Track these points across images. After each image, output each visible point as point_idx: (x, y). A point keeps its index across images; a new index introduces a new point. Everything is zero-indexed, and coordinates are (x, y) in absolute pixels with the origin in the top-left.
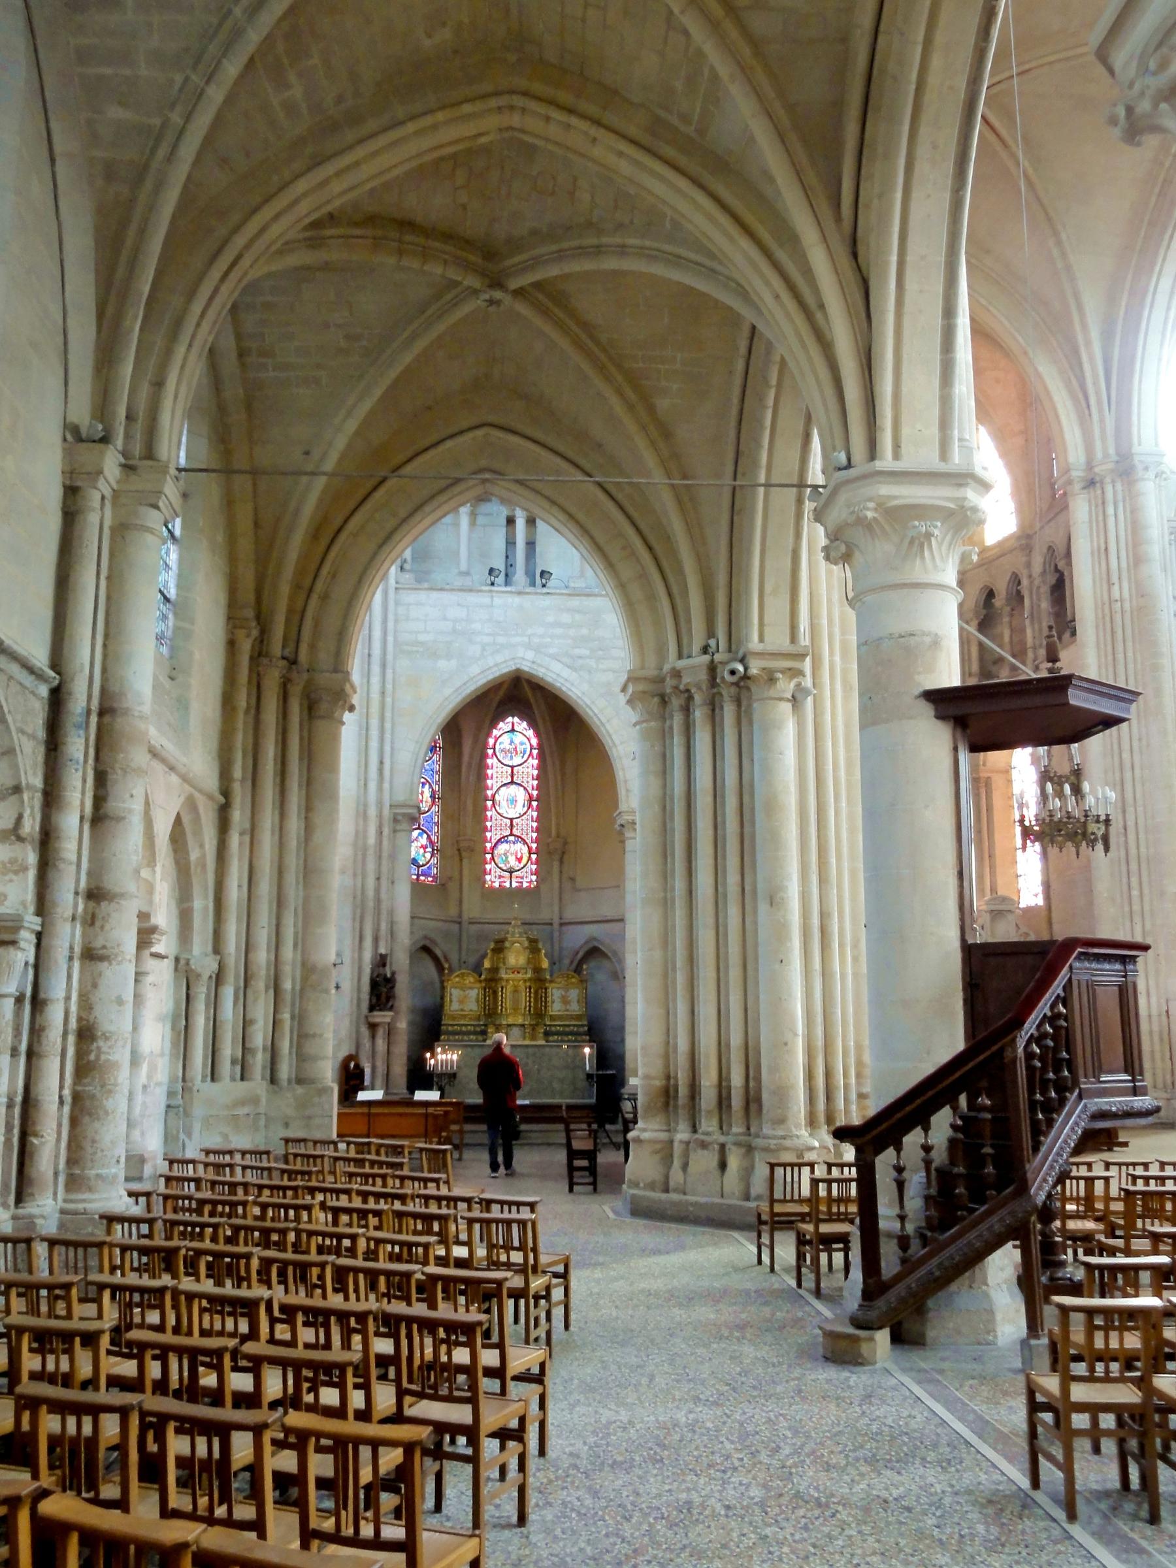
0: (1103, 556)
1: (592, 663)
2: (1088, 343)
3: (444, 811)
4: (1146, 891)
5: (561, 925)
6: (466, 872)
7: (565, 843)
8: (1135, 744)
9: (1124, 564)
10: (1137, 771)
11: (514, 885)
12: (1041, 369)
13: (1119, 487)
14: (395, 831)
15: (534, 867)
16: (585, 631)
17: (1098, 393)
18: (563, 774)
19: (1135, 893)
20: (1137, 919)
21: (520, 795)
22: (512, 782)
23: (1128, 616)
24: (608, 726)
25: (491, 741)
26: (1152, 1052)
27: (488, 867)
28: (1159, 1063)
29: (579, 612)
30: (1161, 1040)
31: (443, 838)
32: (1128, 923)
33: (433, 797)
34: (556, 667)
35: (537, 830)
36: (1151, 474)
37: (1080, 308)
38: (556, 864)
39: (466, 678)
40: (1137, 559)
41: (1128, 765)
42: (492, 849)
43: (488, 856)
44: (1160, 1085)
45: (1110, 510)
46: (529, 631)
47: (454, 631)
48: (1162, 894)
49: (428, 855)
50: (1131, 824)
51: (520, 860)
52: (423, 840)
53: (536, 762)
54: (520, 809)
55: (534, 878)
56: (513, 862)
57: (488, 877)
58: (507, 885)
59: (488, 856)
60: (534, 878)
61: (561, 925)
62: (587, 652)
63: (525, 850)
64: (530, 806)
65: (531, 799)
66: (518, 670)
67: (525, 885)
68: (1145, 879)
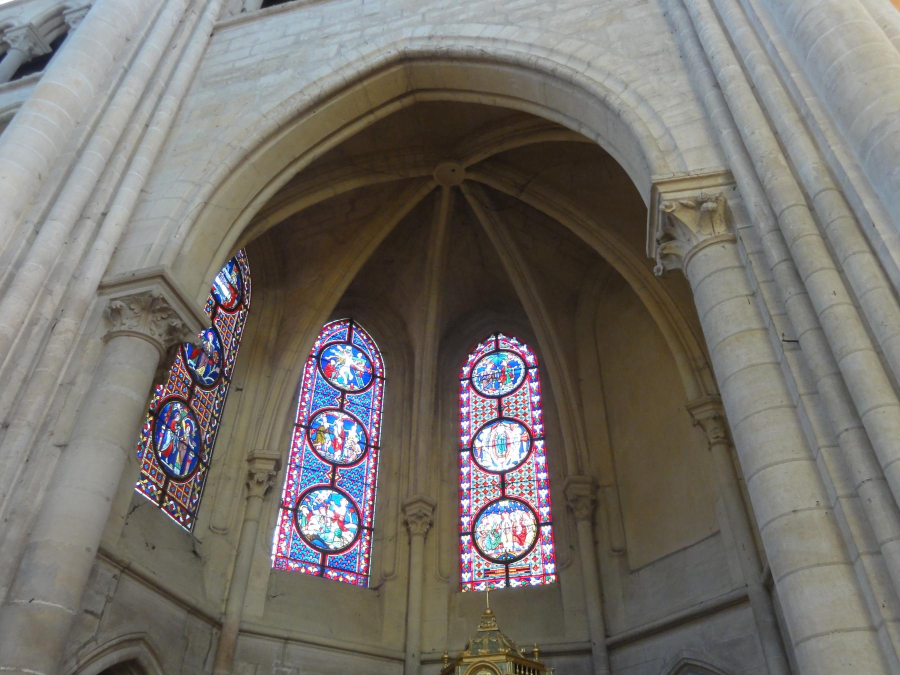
3: (385, 468)
5: (611, 648)
6: (417, 559)
7: (596, 486)
14: (108, 338)
15: (548, 548)
18: (577, 381)
21: (516, 433)
22: (501, 419)
25: (466, 370)
27: (465, 557)
31: (378, 508)
33: (366, 444)
34: (474, 30)
35: (549, 484)
38: (583, 527)
39: (304, 83)
42: (473, 525)
43: (466, 539)
46: (424, 9)
47: (297, 43)
49: (349, 537)
51: (521, 539)
52: (342, 508)
53: (535, 385)
54: (515, 454)
55: (550, 568)
56: (510, 545)
57: (466, 577)
59: (466, 539)
60: (550, 568)
61: (611, 648)
63: (529, 520)
64: (532, 448)
65: (532, 438)
66: (405, 59)
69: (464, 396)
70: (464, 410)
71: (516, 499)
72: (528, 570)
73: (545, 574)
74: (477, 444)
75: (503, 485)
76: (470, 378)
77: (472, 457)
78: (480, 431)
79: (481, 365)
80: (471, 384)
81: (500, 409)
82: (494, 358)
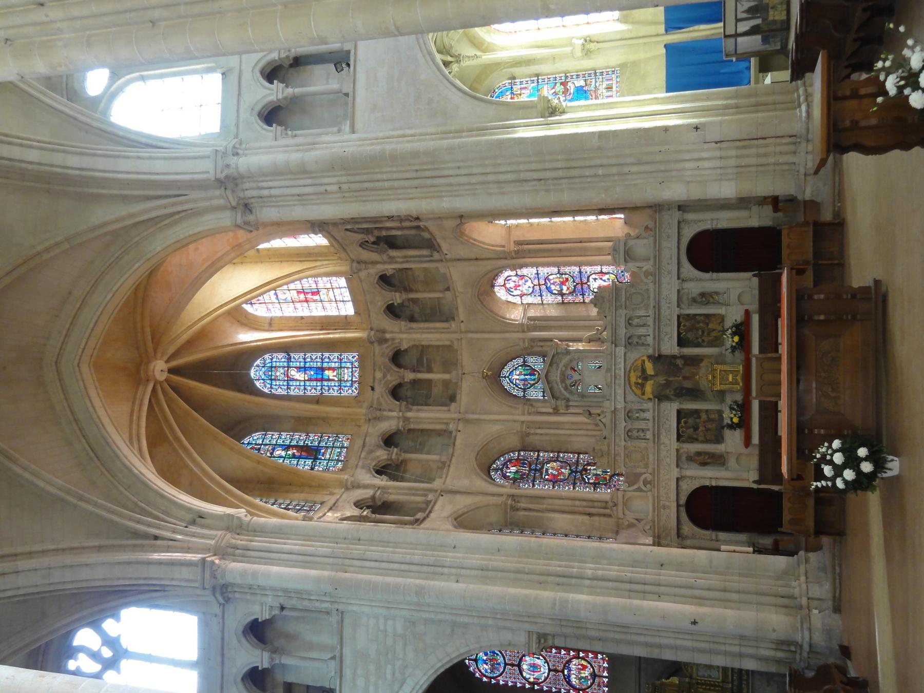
0: (304, 197)
1: (398, 663)
2: (132, 216)
4: (599, 162)
8: (463, 171)
9: (309, 181)
10: (488, 170)
11: (605, 674)
12: (159, 249)
13: (247, 186)
15: (591, 655)
16: (372, 667)
17: (173, 205)
19: (600, 172)
20: (625, 169)
22: (519, 666)
23: (351, 178)
24: (453, 656)
25: (485, 679)
26: (758, 156)
28: (770, 149)
29: (355, 670)
30: (744, 147)
32: (630, 177)
36: (232, 160)
37: (101, 226)
40: (302, 171)
41: (481, 178)
44: (792, 148)
45: (266, 192)
48: (599, 148)
50: (536, 175)
51: (584, 667)
56: (586, 673)
58: (606, 680)
62: (389, 667)
63: (575, 661)
67: (606, 665)
68: (587, 163)
69: (501, 683)
70: (510, 684)
71: (565, 666)
72: (600, 666)
73: (602, 659)
74: (532, 680)
75: (556, 671)
76: (491, 678)
77: (538, 684)
78: (525, 678)
79: (483, 671)
80: (494, 678)
81: (513, 665)
82: (480, 663)
